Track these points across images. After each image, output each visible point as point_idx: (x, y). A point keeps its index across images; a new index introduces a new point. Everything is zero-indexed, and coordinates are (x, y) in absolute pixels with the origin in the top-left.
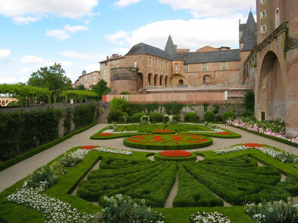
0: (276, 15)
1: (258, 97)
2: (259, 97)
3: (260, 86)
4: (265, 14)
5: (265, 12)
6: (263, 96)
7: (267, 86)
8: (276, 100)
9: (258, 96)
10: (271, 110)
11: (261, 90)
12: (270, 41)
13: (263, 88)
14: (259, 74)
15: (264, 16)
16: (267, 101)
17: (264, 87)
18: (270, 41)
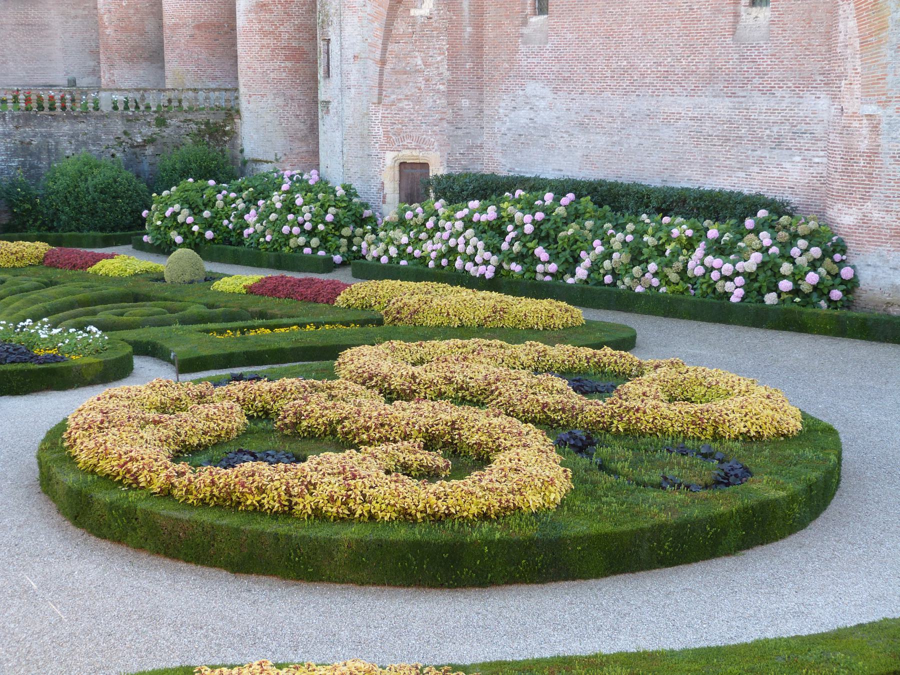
1: (381, 74)
2: (388, 66)
6: (419, 62)
9: (383, 62)
10: (468, 148)
11: (400, 27)
13: (413, 12)
16: (450, 93)
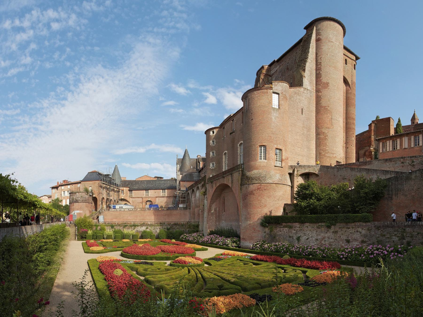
0: (224, 157)
3: (210, 210)
4: (215, 154)
5: (215, 152)
7: (215, 210)
8: (223, 221)
11: (210, 214)
12: (224, 176)
14: (209, 201)
15: (213, 155)
17: (213, 211)
18: (224, 176)
